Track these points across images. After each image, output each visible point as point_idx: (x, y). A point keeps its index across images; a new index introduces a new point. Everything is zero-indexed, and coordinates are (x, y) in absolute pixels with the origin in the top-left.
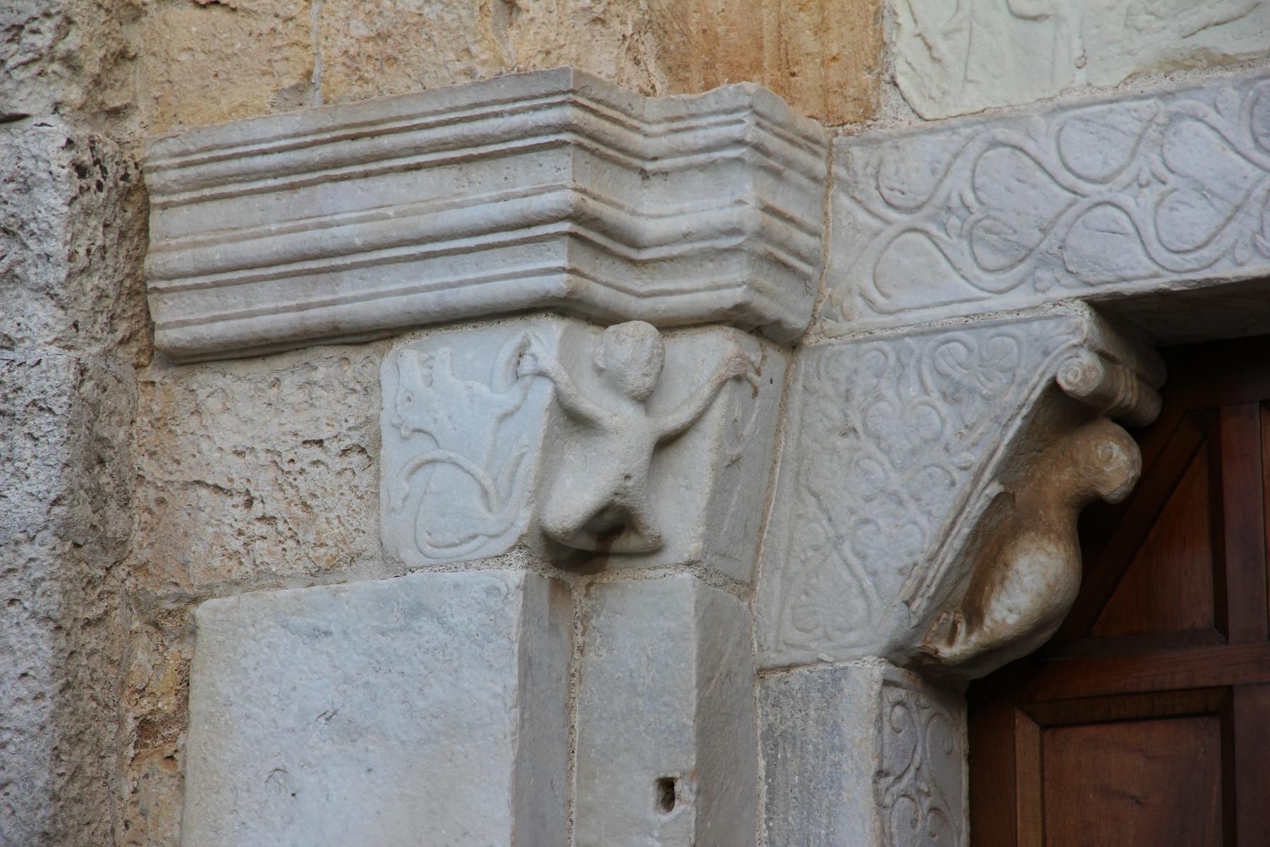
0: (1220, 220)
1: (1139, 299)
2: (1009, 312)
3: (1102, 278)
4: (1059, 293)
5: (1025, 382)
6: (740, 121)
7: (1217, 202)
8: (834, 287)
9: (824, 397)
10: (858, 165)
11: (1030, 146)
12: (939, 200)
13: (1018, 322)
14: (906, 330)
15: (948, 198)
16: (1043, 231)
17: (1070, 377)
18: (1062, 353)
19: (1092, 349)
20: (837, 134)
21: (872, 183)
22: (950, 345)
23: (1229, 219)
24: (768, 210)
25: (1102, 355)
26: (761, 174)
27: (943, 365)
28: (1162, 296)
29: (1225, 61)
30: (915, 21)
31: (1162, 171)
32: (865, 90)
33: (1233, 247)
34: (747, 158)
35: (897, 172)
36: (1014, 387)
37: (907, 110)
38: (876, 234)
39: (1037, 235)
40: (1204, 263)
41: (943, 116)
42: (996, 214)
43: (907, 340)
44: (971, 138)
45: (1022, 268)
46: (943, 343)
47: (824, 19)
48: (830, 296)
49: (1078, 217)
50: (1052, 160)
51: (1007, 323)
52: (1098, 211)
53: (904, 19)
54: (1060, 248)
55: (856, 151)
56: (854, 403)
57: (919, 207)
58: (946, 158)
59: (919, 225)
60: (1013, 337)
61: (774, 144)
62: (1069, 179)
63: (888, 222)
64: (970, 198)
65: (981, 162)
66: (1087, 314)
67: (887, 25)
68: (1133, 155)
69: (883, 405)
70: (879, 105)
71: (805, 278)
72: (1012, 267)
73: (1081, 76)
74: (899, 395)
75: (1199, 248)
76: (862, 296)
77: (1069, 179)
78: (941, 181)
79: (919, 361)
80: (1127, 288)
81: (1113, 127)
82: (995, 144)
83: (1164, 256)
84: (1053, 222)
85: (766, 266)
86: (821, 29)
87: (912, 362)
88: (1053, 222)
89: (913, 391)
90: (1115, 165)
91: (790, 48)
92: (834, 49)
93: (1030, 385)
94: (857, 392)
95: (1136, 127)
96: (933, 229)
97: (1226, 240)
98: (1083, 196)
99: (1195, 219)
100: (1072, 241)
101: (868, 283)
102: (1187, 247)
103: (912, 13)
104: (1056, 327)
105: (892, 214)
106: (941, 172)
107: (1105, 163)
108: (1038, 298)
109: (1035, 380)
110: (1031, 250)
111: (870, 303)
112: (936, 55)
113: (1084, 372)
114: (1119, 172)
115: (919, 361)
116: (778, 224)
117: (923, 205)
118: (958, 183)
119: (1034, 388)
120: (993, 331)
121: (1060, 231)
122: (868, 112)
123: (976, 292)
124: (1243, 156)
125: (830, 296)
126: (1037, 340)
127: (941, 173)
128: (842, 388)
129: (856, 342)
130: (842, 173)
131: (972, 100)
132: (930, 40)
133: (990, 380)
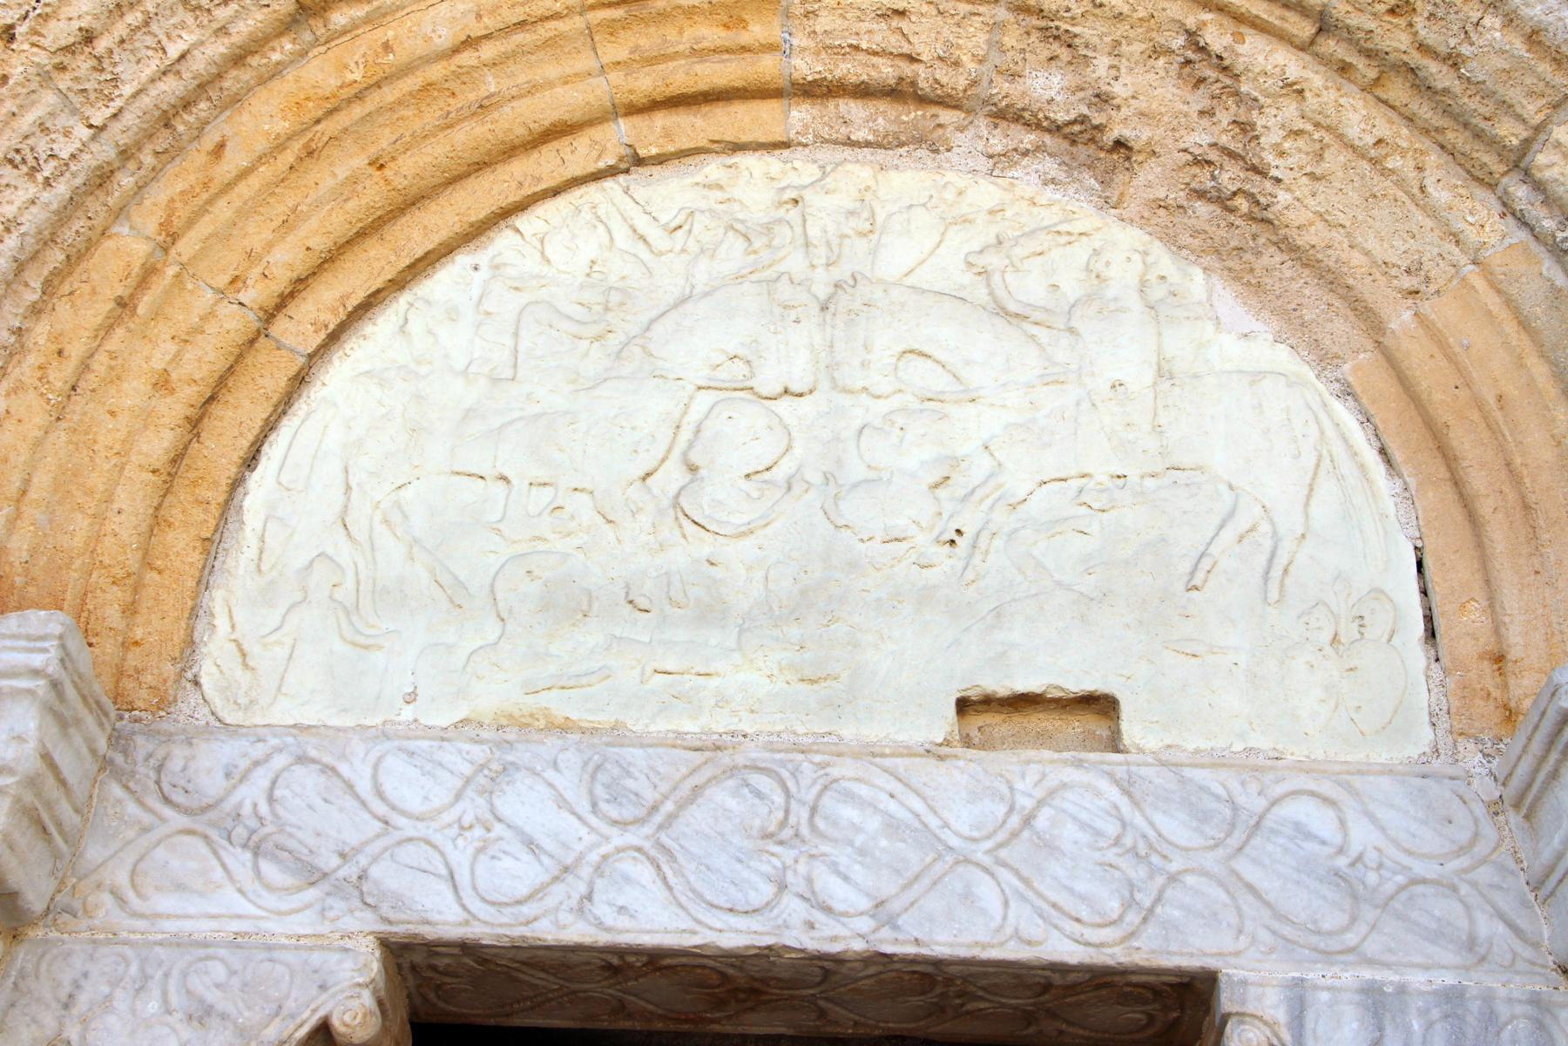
0: (546, 878)
1: (432, 948)
2: (289, 937)
3: (403, 917)
4: (350, 923)
5: (292, 1016)
6: (45, 650)
7: (546, 860)
8: (80, 880)
9: (38, 1000)
10: (140, 755)
11: (344, 769)
12: (228, 806)
13: (297, 948)
14: (160, 936)
15: (240, 804)
16: (343, 855)
17: (347, 1018)
18: (342, 991)
19: (375, 992)
20: (121, 718)
21: (152, 774)
22: (209, 963)
23: (556, 879)
24: (47, 757)
25: (380, 1003)
26: (49, 719)
27: (196, 983)
28: (467, 948)
29: (565, 727)
30: (233, 627)
31: (489, 816)
32: (165, 681)
33: (557, 909)
34: (41, 692)
35: (184, 769)
36: (277, 1020)
37: (206, 710)
38: (145, 830)
39: (335, 861)
40: (522, 919)
41: (247, 723)
42: (293, 830)
43: (158, 949)
44: (280, 750)
45: (311, 894)
46: (201, 960)
47: (134, 602)
48: (74, 887)
49: (386, 849)
50: (364, 786)
51: (283, 947)
52: (410, 847)
53: (222, 622)
54: (360, 878)
55: (140, 740)
56: (75, 1011)
57: (205, 809)
58: (244, 764)
59: (199, 827)
60: (288, 965)
61: (71, 692)
62: (381, 809)
63: (163, 820)
64: (264, 809)
65: (286, 774)
66: (377, 953)
67: (200, 626)
68: (458, 796)
69: (111, 1020)
70: (175, 701)
71: (56, 855)
72: (299, 889)
73: (408, 713)
74: (133, 1011)
75: (519, 902)
76: (112, 892)
77: (381, 809)
78: (234, 787)
79: (166, 975)
80: (430, 933)
81: (441, 764)
82: (302, 759)
83: (476, 906)
84: (357, 851)
85: (25, 823)
86: (130, 610)
87: (159, 975)
88: (357, 851)
89: (153, 1006)
90: (437, 802)
91: (93, 618)
92: (139, 633)
93: (298, 1021)
94: (83, 999)
95: (467, 769)
96: (214, 834)
97: (550, 902)
98: (396, 828)
99: (515, 873)
100: (374, 872)
101: (122, 878)
102: (504, 900)
103: (231, 617)
104: (340, 962)
105: (168, 812)
106: (237, 777)
107: (426, 798)
108: (325, 928)
109: (305, 1015)
110: (325, 875)
111: (121, 901)
112: (251, 664)
113: (365, 1015)
114: (440, 811)
115: (166, 975)
116: (50, 781)
117: (209, 807)
118: (251, 794)
119: (301, 1025)
120: (263, 955)
121: (363, 860)
122: (163, 703)
123: (253, 910)
124: (580, 818)
125: (74, 887)
126: (315, 972)
127: (236, 776)
128: (63, 995)
129: (94, 942)
130: (119, 759)
131: (284, 712)
132: (245, 647)
133: (249, 1008)
